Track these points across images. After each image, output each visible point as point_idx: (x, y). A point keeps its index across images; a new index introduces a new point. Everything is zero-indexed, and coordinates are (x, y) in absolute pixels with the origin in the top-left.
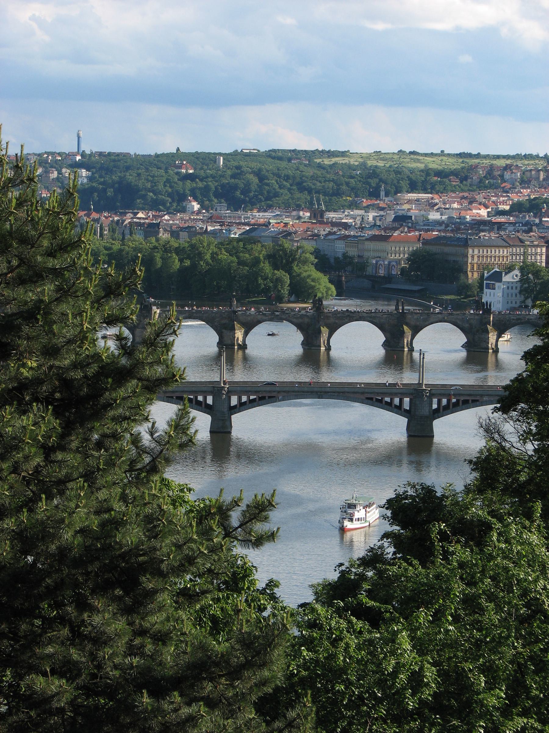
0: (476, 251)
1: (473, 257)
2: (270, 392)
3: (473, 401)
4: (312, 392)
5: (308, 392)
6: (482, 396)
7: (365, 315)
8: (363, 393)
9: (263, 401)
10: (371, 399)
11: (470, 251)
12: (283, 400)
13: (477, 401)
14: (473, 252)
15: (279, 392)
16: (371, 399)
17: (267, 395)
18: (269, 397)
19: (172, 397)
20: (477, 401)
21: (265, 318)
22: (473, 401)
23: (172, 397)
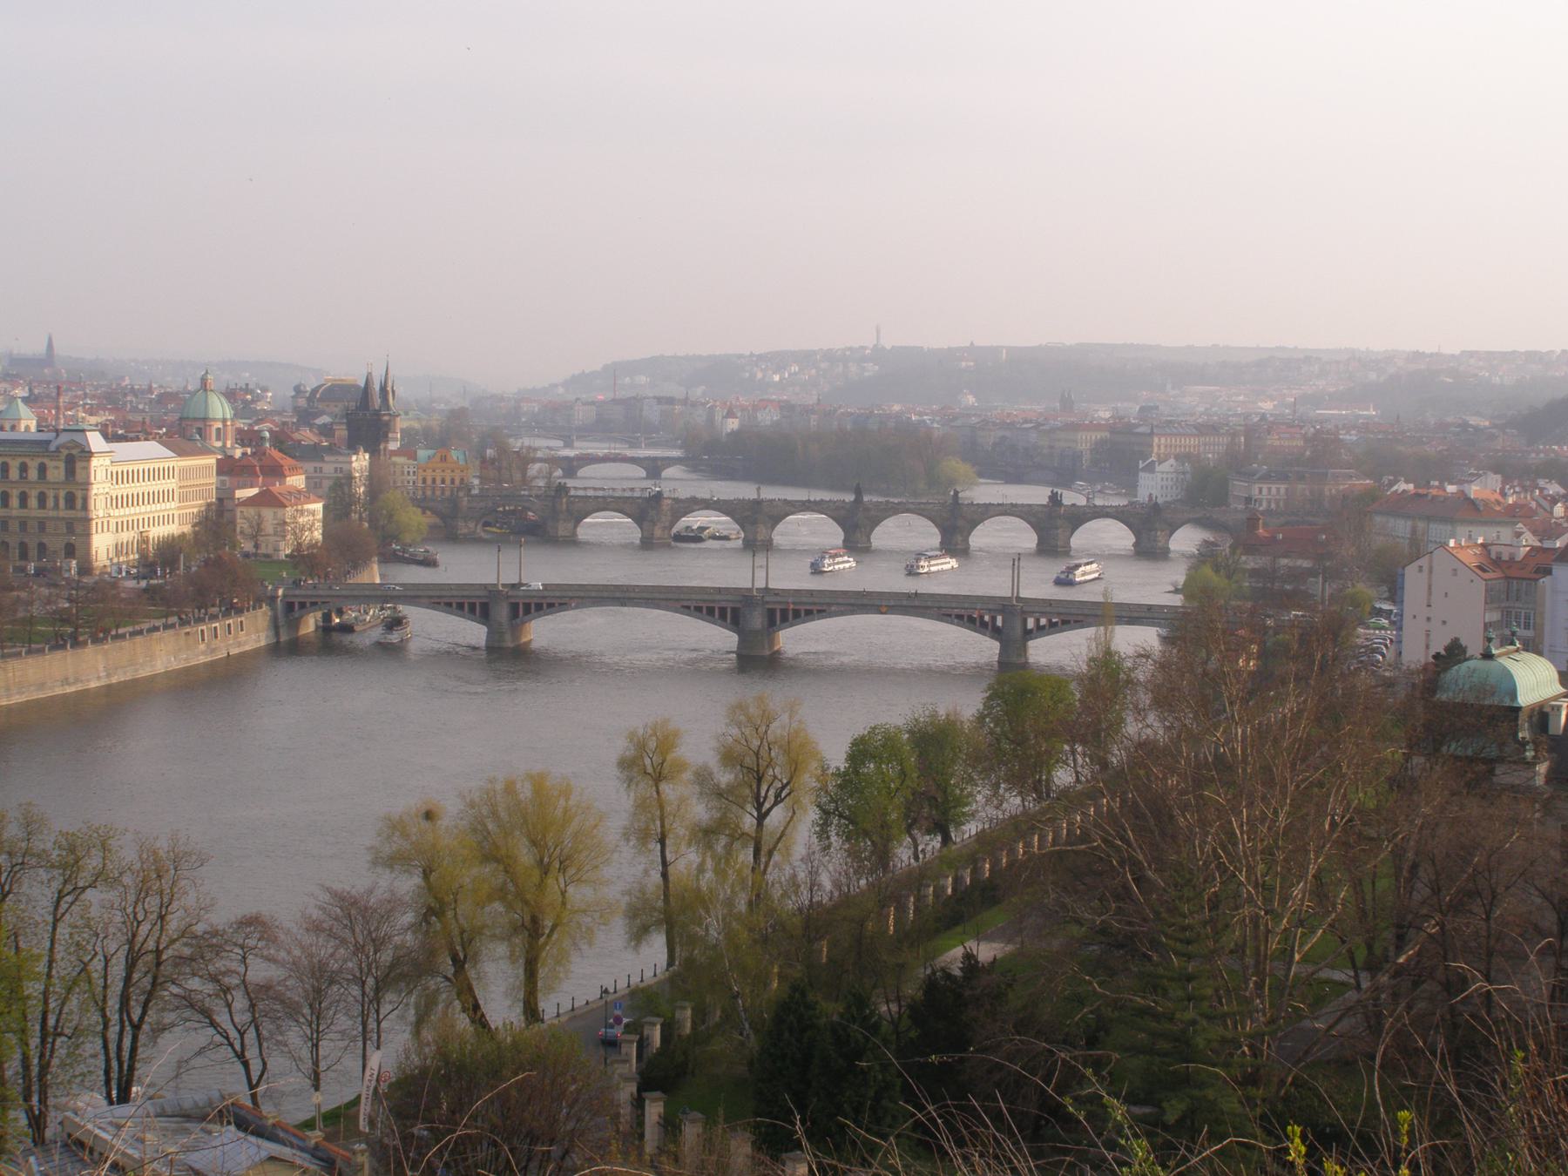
0: (1163, 440)
1: (1159, 446)
2: (558, 597)
3: (819, 611)
4: (613, 598)
5: (608, 598)
6: (830, 605)
7: (912, 506)
8: (677, 600)
9: (552, 609)
10: (688, 607)
11: (1156, 440)
12: (577, 607)
13: (824, 611)
14: (1160, 440)
15: (571, 598)
16: (688, 607)
17: (556, 601)
18: (561, 604)
19: (439, 603)
20: (824, 611)
21: (793, 509)
22: (819, 611)
23: (439, 603)
